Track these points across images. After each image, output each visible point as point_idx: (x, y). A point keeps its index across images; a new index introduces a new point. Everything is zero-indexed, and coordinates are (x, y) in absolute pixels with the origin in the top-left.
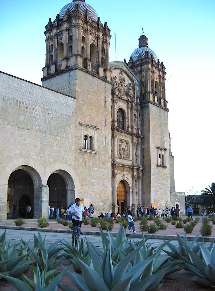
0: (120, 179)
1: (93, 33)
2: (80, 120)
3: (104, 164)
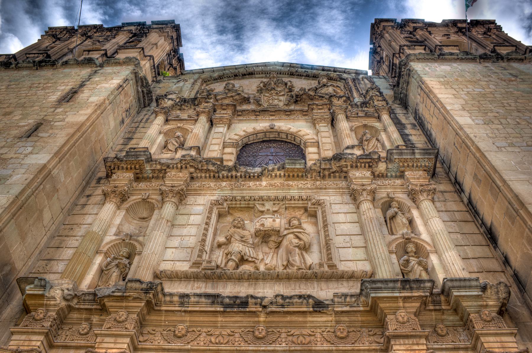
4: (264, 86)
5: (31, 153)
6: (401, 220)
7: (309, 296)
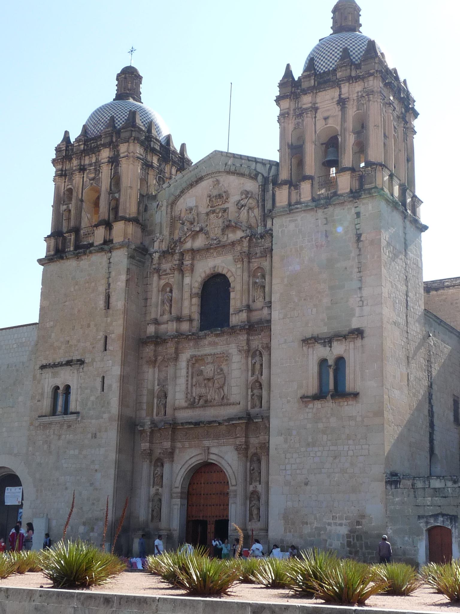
0: (190, 462)
1: (90, 165)
2: (44, 362)
3: (95, 436)
4: (210, 200)
5: (112, 366)
6: (258, 366)
7: (216, 421)
